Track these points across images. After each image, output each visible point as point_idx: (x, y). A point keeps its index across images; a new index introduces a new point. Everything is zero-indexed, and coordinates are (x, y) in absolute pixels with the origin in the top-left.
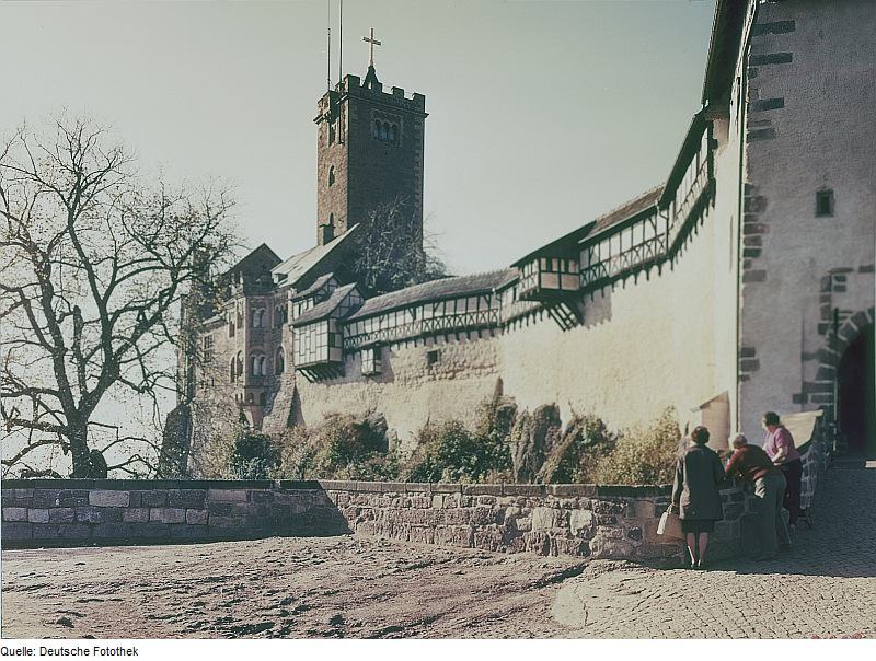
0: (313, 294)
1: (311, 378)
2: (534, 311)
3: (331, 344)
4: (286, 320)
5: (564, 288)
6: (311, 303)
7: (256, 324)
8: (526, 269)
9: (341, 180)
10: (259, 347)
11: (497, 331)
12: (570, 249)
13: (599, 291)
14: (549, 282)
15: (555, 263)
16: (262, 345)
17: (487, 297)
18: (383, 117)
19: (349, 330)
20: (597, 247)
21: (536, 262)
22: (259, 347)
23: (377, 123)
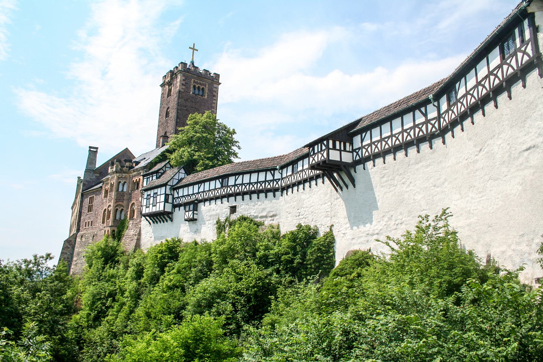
0: (157, 172)
1: (151, 221)
2: (318, 177)
3: (166, 201)
4: (138, 188)
5: (343, 160)
6: (154, 178)
7: (120, 190)
8: (316, 147)
9: (173, 114)
10: (121, 203)
11: (278, 194)
12: (346, 134)
13: (372, 162)
14: (334, 156)
15: (338, 143)
16: (123, 202)
17: (272, 172)
18: (197, 83)
19: (178, 193)
20: (369, 132)
21: (325, 142)
22: (121, 203)
23: (194, 87)
